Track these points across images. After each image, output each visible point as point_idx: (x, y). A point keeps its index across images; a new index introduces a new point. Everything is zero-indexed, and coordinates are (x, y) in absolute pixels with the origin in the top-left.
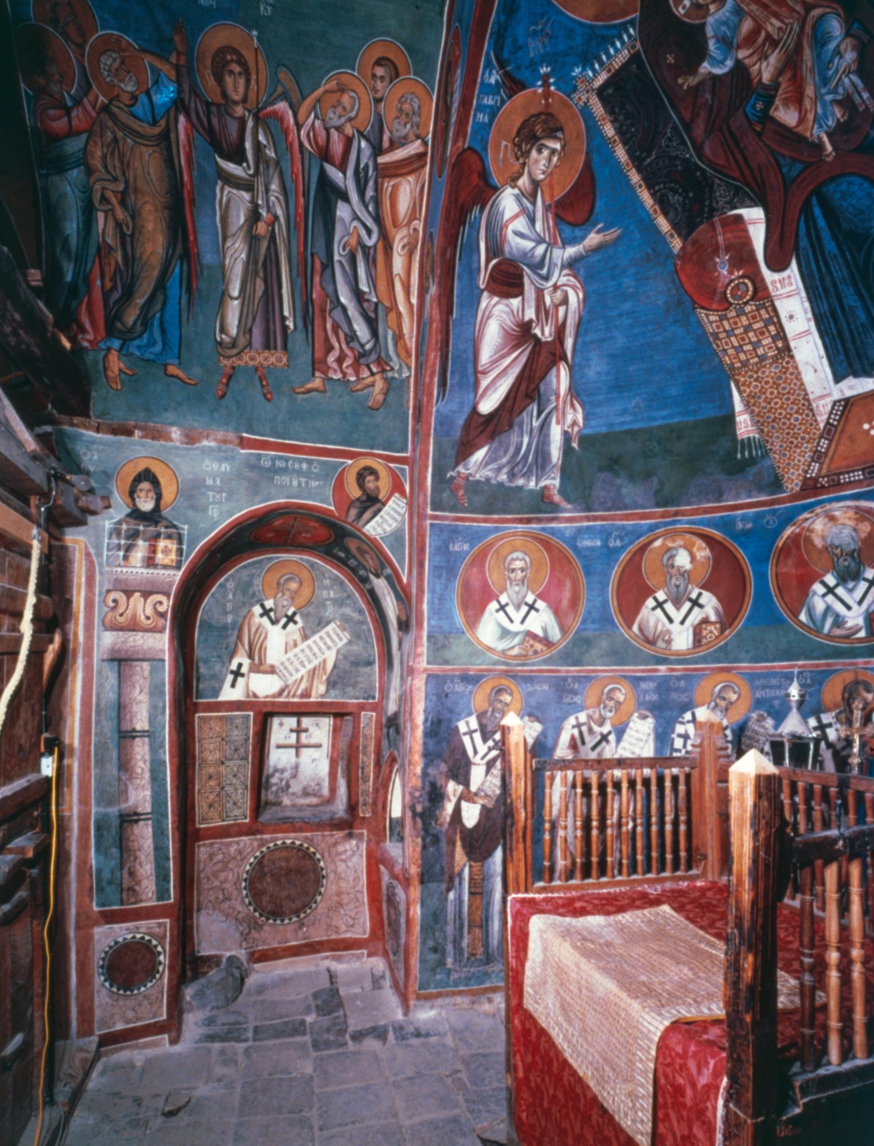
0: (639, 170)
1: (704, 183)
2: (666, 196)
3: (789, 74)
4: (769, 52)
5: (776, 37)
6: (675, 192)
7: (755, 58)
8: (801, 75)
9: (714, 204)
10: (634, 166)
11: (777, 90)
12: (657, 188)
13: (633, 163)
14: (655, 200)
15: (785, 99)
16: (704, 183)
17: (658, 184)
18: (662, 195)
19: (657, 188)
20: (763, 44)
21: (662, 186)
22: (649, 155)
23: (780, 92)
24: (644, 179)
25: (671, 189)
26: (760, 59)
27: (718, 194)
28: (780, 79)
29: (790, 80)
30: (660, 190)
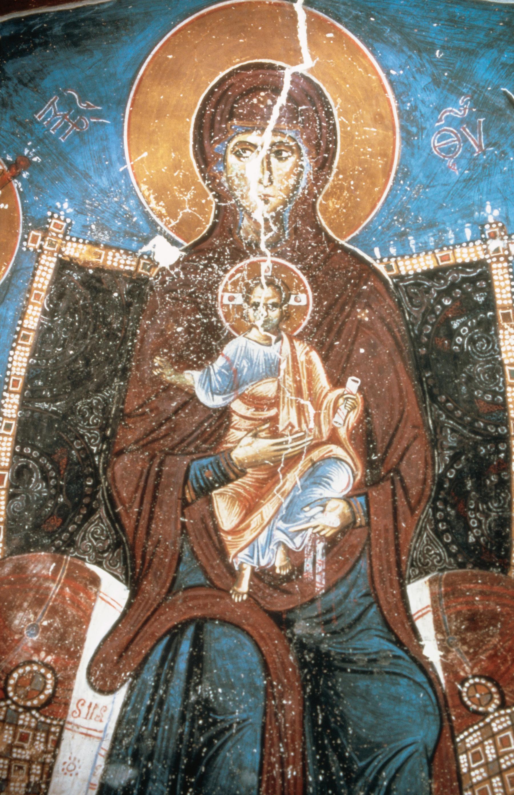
0: (23, 405)
1: (86, 501)
2: (31, 472)
3: (261, 475)
4: (263, 434)
5: (281, 427)
6: (46, 479)
7: (246, 424)
8: (270, 490)
9: (78, 538)
10: (22, 394)
11: (238, 477)
12: (27, 450)
13: (24, 389)
14: (11, 463)
15: (238, 494)
16: (86, 501)
17: (34, 447)
18: (25, 467)
19: (27, 450)
20: (265, 421)
21: (35, 454)
22: (54, 399)
23: (239, 481)
24: (20, 422)
25: (43, 470)
26: (249, 431)
27: (92, 529)
28: (249, 470)
29: (257, 480)
30: (28, 457)
